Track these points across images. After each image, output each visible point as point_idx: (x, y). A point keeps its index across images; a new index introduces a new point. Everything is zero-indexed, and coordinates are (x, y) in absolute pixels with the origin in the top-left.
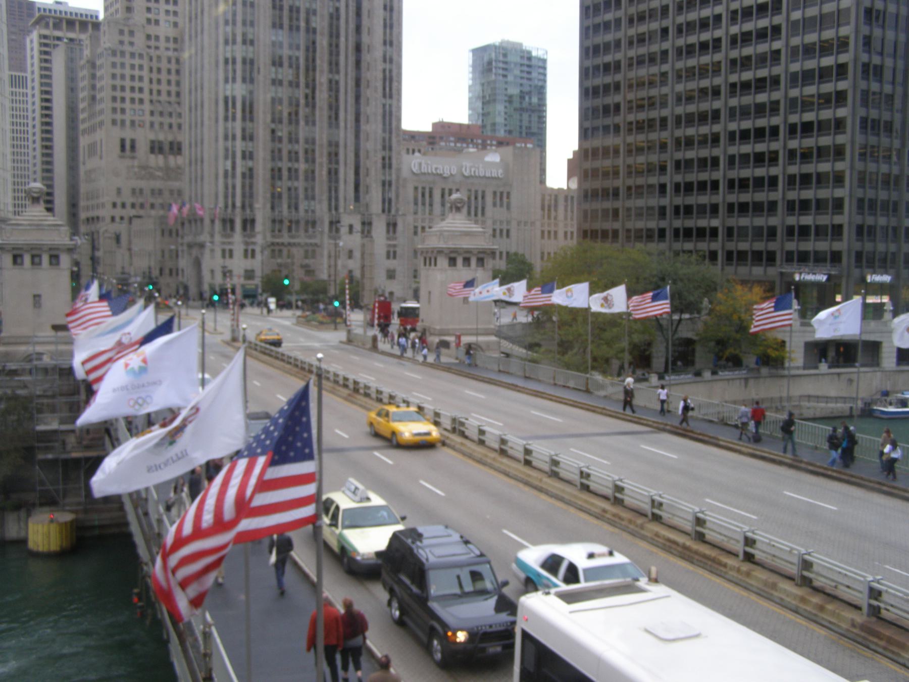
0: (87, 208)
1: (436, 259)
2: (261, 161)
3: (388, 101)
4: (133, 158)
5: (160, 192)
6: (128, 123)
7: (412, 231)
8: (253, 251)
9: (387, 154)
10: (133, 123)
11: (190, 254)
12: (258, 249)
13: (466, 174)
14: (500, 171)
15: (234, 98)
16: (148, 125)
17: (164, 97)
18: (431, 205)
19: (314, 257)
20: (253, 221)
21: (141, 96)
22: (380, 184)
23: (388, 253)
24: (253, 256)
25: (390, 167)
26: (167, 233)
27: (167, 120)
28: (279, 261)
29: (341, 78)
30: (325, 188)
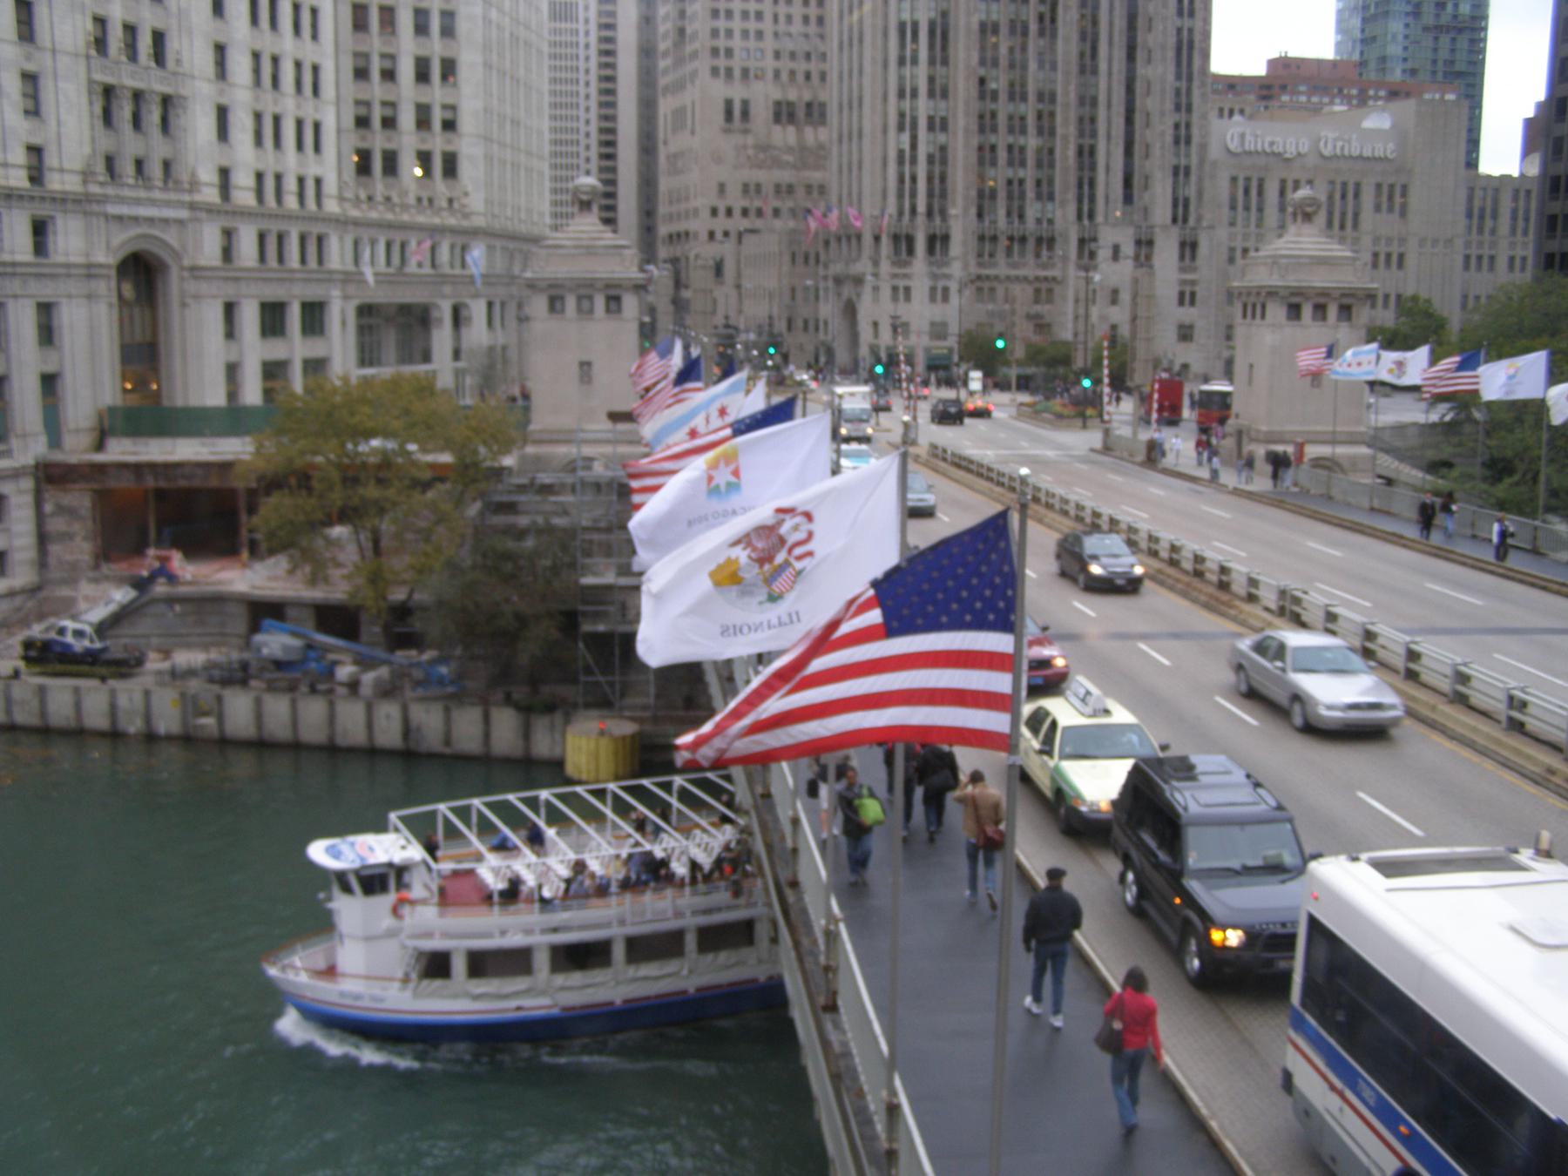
0: (670, 218)
1: (1264, 307)
2: (960, 133)
3: (1187, 23)
4: (746, 132)
5: (790, 189)
6: (737, 73)
7: (1225, 257)
8: (946, 290)
9: (1183, 117)
10: (745, 72)
11: (839, 295)
12: (954, 286)
13: (1327, 152)
14: (1391, 146)
15: (915, 25)
16: (770, 75)
17: (797, 27)
18: (1260, 210)
19: (1050, 301)
20: (946, 238)
21: (760, 26)
22: (1169, 173)
23: (1182, 295)
24: (946, 298)
25: (1188, 142)
26: (800, 260)
27: (801, 66)
28: (990, 307)
30: (1073, 180)
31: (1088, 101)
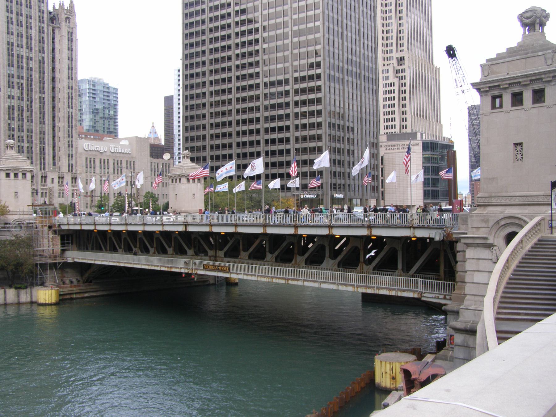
1: (180, 179)
3: (71, 110)
9: (71, 139)
22: (67, 156)
25: (72, 147)
29: (46, 96)
30: (39, 158)
31: (42, 133)
